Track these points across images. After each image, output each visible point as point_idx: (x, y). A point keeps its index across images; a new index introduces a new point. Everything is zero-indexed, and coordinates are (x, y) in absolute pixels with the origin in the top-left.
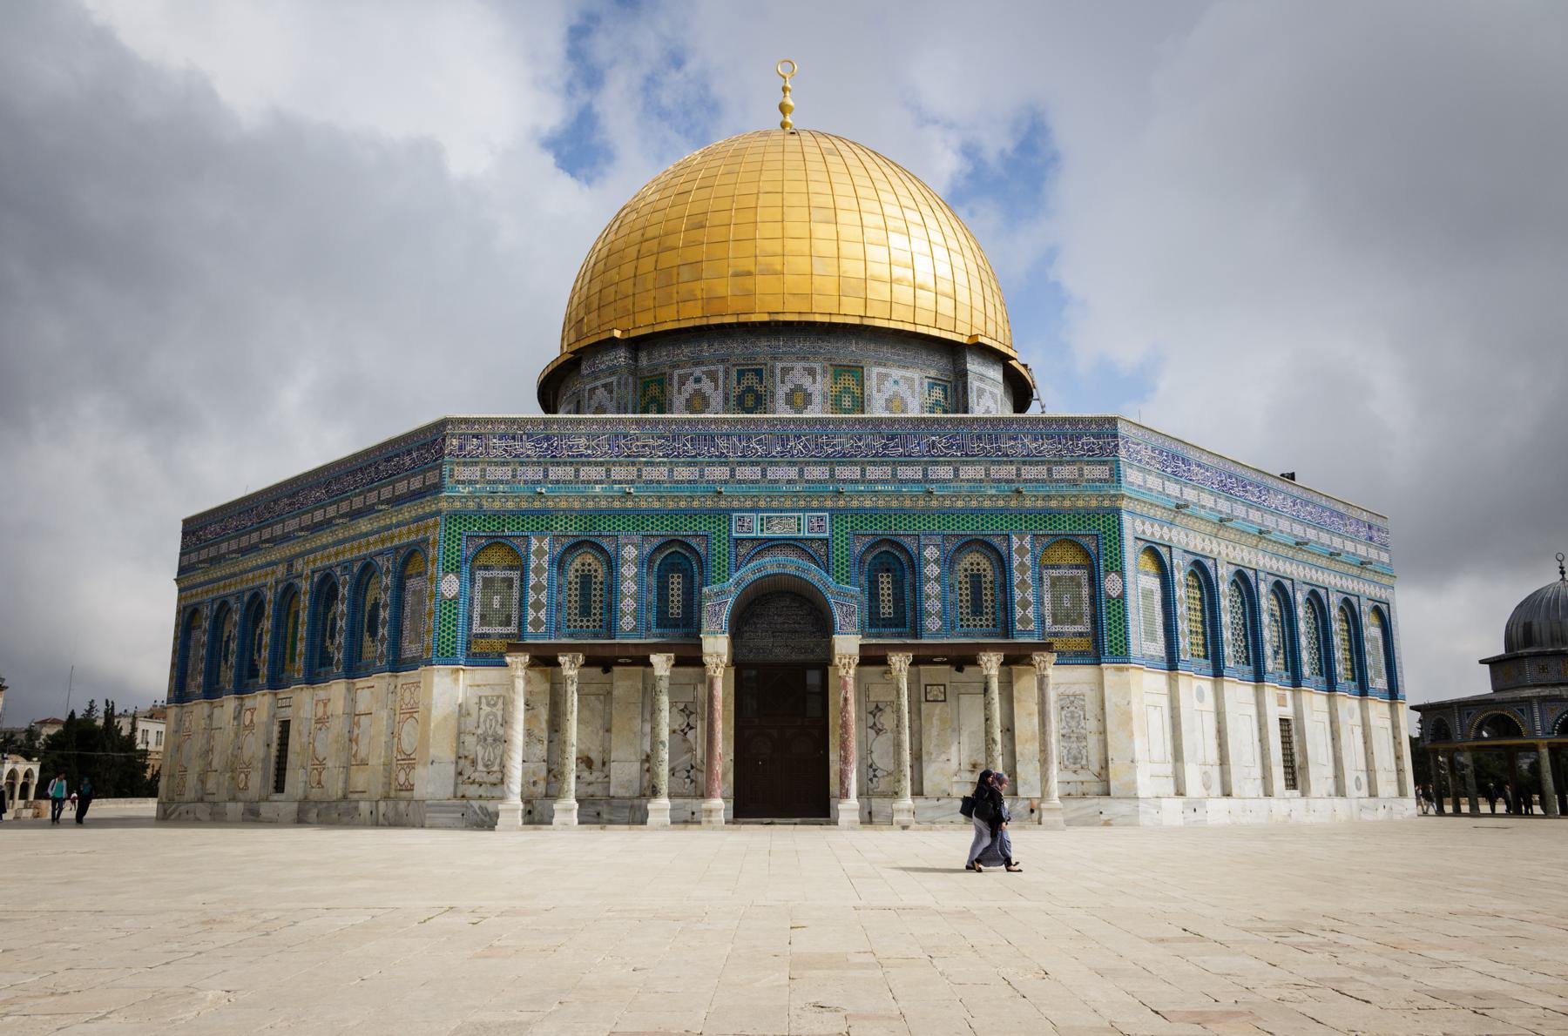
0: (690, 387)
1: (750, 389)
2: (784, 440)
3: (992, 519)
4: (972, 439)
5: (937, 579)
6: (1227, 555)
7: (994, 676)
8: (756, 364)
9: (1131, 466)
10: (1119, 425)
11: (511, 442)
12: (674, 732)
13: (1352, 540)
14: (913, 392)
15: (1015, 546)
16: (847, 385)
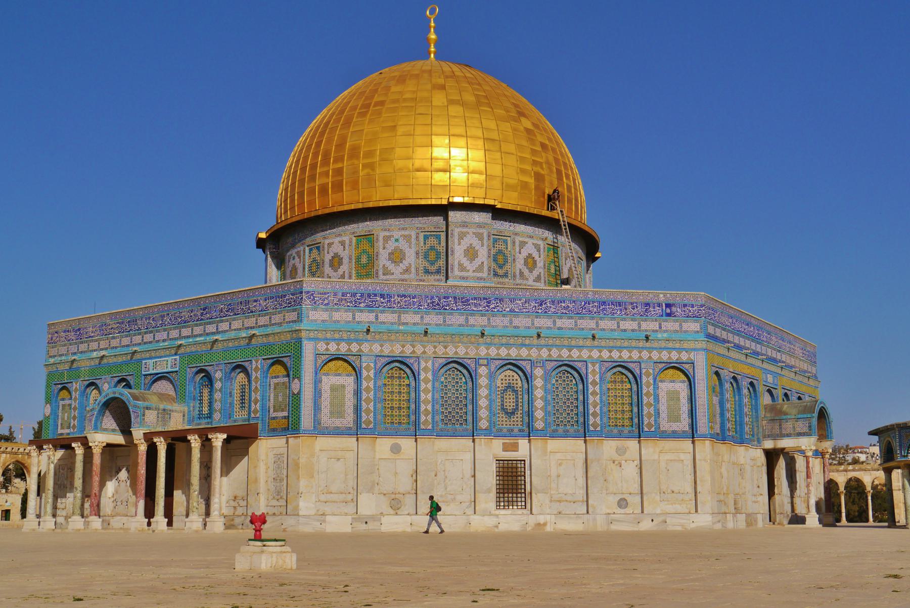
0: (292, 262)
1: (314, 260)
2: (163, 317)
3: (245, 352)
4: (238, 305)
5: (220, 390)
6: (435, 352)
7: (195, 447)
8: (317, 244)
9: (315, 309)
10: (304, 285)
11: (67, 333)
12: (123, 481)
13: (632, 320)
14: (410, 244)
15: (254, 367)
16: (365, 248)
